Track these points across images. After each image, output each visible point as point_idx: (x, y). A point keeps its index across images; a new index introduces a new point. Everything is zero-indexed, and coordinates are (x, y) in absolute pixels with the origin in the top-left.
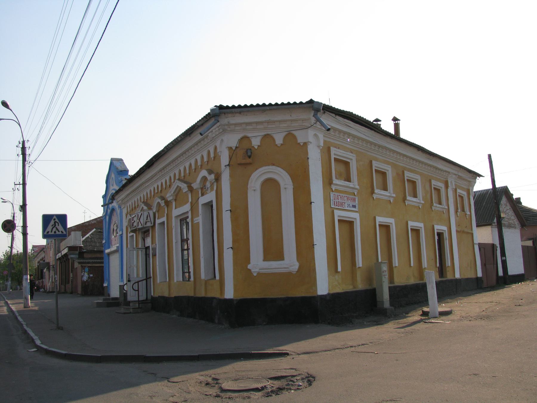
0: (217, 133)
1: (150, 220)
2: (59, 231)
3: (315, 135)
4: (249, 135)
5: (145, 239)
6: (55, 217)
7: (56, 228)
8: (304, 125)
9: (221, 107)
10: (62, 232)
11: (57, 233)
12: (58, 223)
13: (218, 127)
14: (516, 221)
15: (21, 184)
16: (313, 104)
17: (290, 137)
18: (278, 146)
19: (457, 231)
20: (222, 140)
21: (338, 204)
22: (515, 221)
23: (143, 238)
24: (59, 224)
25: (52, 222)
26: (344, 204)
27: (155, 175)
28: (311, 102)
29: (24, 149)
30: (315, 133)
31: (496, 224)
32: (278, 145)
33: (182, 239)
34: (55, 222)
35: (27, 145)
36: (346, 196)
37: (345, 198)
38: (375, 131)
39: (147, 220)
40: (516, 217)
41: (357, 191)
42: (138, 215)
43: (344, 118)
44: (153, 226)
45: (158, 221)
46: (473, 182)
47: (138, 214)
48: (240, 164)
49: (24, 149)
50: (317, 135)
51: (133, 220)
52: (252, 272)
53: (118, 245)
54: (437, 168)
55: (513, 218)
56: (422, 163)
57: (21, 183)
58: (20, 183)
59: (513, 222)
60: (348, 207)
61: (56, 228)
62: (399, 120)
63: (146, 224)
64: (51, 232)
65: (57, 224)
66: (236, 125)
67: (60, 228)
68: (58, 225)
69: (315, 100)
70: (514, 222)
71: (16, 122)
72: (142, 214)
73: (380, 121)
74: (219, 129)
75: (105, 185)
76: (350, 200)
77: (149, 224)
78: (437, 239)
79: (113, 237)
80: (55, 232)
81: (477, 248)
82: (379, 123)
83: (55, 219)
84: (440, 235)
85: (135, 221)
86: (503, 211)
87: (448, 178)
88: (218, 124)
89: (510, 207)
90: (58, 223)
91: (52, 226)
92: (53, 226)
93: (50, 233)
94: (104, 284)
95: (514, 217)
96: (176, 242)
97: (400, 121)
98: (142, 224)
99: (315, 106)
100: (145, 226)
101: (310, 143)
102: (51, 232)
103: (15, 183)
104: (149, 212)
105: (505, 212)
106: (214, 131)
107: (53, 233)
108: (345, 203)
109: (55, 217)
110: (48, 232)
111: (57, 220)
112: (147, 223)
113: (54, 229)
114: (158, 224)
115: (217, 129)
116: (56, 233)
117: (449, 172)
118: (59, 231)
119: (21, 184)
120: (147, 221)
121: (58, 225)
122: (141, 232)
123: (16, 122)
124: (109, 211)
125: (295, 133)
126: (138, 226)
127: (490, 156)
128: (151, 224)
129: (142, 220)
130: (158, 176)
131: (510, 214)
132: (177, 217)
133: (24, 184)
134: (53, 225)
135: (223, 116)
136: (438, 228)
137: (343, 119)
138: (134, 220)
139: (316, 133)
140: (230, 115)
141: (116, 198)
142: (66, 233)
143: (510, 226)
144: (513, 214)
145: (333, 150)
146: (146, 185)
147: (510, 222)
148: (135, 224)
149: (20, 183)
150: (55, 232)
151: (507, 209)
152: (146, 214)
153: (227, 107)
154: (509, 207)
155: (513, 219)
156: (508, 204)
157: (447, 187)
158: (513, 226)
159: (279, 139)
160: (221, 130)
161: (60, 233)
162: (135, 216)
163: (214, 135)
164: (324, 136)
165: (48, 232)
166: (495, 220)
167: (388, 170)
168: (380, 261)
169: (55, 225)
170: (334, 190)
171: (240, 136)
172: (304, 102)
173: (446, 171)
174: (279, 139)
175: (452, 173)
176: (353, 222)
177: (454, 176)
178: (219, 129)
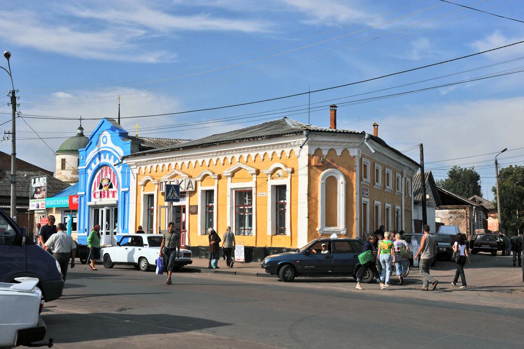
4: (321, 148)
6: (173, 187)
11: (174, 198)
17: (345, 151)
19: (405, 210)
25: (171, 190)
35: (16, 95)
54: (400, 164)
56: (394, 160)
63: (187, 189)
66: (316, 141)
73: (336, 107)
81: (413, 222)
100: (186, 190)
113: (172, 195)
125: (348, 149)
127: (421, 145)
133: (14, 133)
140: (313, 135)
143: (429, 206)
152: (187, 181)
157: (402, 177)
159: (339, 153)
161: (176, 198)
171: (316, 148)
173: (405, 166)
174: (339, 153)
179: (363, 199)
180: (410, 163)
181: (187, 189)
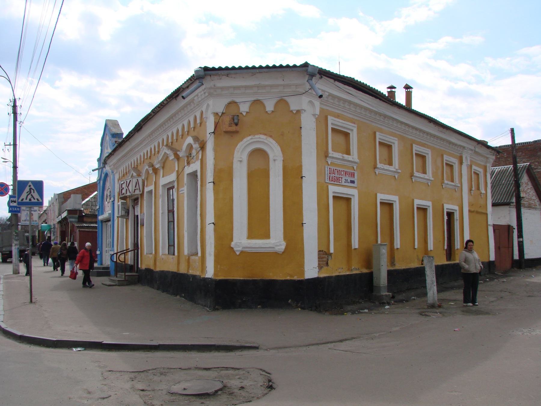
0: (203, 97)
1: (139, 188)
2: (34, 199)
3: (310, 102)
4: (237, 100)
5: (135, 207)
6: (30, 184)
7: (32, 195)
8: (298, 91)
9: (206, 69)
10: (38, 200)
11: (33, 200)
12: (34, 190)
13: (203, 90)
14: (537, 201)
15: (11, 145)
16: (306, 68)
17: (282, 103)
18: (269, 114)
19: (470, 211)
20: (208, 105)
21: (334, 179)
22: (536, 201)
23: (133, 206)
24: (35, 191)
25: (27, 189)
26: (340, 179)
27: (144, 140)
28: (306, 65)
29: (15, 107)
30: (310, 99)
31: (515, 204)
32: (268, 112)
33: (169, 209)
34: (31, 189)
35: (18, 104)
36: (344, 171)
37: (342, 173)
38: (380, 99)
39: (135, 187)
40: (537, 197)
41: (357, 165)
42: (127, 181)
43: (345, 84)
44: (142, 195)
45: (146, 190)
46: (490, 158)
47: (126, 180)
48: (226, 132)
49: (15, 107)
50: (313, 102)
51: (122, 187)
52: (235, 251)
53: (110, 212)
54: (450, 143)
55: (534, 198)
56: (434, 136)
57: (12, 143)
58: (10, 143)
59: (533, 202)
60: (345, 182)
61: (32, 195)
62: (412, 88)
63: (134, 192)
64: (26, 199)
65: (32, 191)
66: (222, 88)
67: (36, 195)
68: (34, 192)
69: (311, 63)
70: (535, 203)
71: (7, 79)
72: (130, 181)
73: (395, 88)
74: (205, 93)
75: (100, 148)
76: (348, 175)
77: (137, 192)
78: (447, 220)
79: (107, 203)
80: (30, 200)
81: (491, 229)
82: (393, 90)
83: (30, 186)
84: (450, 215)
85: (123, 188)
86: (524, 191)
87: (463, 153)
88: (203, 87)
89: (532, 187)
90: (34, 190)
91: (27, 193)
92: (29, 193)
93: (25, 201)
94: (97, 252)
95: (536, 197)
96: (162, 213)
97: (412, 89)
98: (131, 192)
99: (310, 69)
100: (133, 194)
101: (303, 111)
102: (26, 199)
103: (5, 143)
104: (137, 179)
105: (526, 191)
106: (199, 94)
107: (28, 200)
108: (342, 178)
109: (30, 184)
110: (23, 200)
111: (32, 187)
112: (136, 190)
113: (30, 197)
114: (147, 192)
115: (203, 92)
116: (31, 201)
117: (464, 148)
118: (34, 199)
119: (11, 145)
120: (136, 188)
121: (34, 192)
122: (131, 199)
123: (7, 79)
124: (103, 175)
125: (287, 99)
126: (126, 193)
127: (512, 131)
128: (140, 191)
129: (130, 187)
130: (147, 141)
131: (530, 193)
132: (164, 186)
133: (15, 145)
134: (28, 192)
135: (208, 78)
136: (448, 207)
137: (343, 85)
138: (123, 187)
139: (312, 100)
140: (216, 77)
141: (108, 162)
142: (41, 201)
143: (530, 207)
144: (535, 194)
145: (330, 119)
146: (137, 150)
147: (531, 202)
148: (124, 191)
149: (10, 143)
150: (30, 200)
151: (528, 189)
152: (135, 181)
153: (214, 69)
154: (530, 186)
155: (534, 200)
156: (530, 183)
157: (461, 163)
158: (534, 206)
159: (270, 106)
160: (207, 94)
161: (36, 201)
162: (124, 182)
163: (200, 99)
164: (320, 103)
165: (23, 200)
166: (514, 200)
167: (394, 143)
168: (379, 242)
169: (30, 192)
170: (329, 163)
171: (226, 101)
172: (298, 65)
173: (461, 146)
174: (270, 106)
175: (468, 148)
176: (350, 199)
177: (470, 152)
178: (205, 93)
179: (333, 189)
180: (426, 122)
181: (134, 192)
